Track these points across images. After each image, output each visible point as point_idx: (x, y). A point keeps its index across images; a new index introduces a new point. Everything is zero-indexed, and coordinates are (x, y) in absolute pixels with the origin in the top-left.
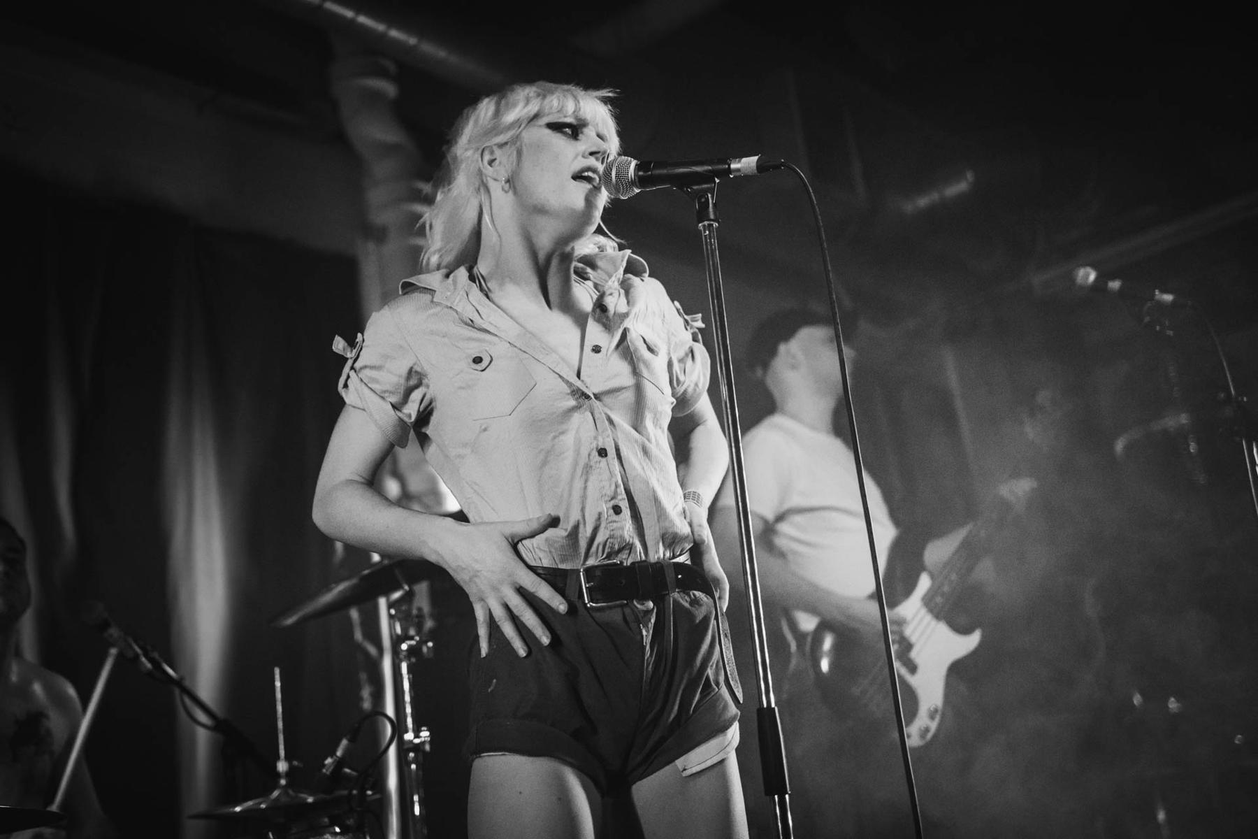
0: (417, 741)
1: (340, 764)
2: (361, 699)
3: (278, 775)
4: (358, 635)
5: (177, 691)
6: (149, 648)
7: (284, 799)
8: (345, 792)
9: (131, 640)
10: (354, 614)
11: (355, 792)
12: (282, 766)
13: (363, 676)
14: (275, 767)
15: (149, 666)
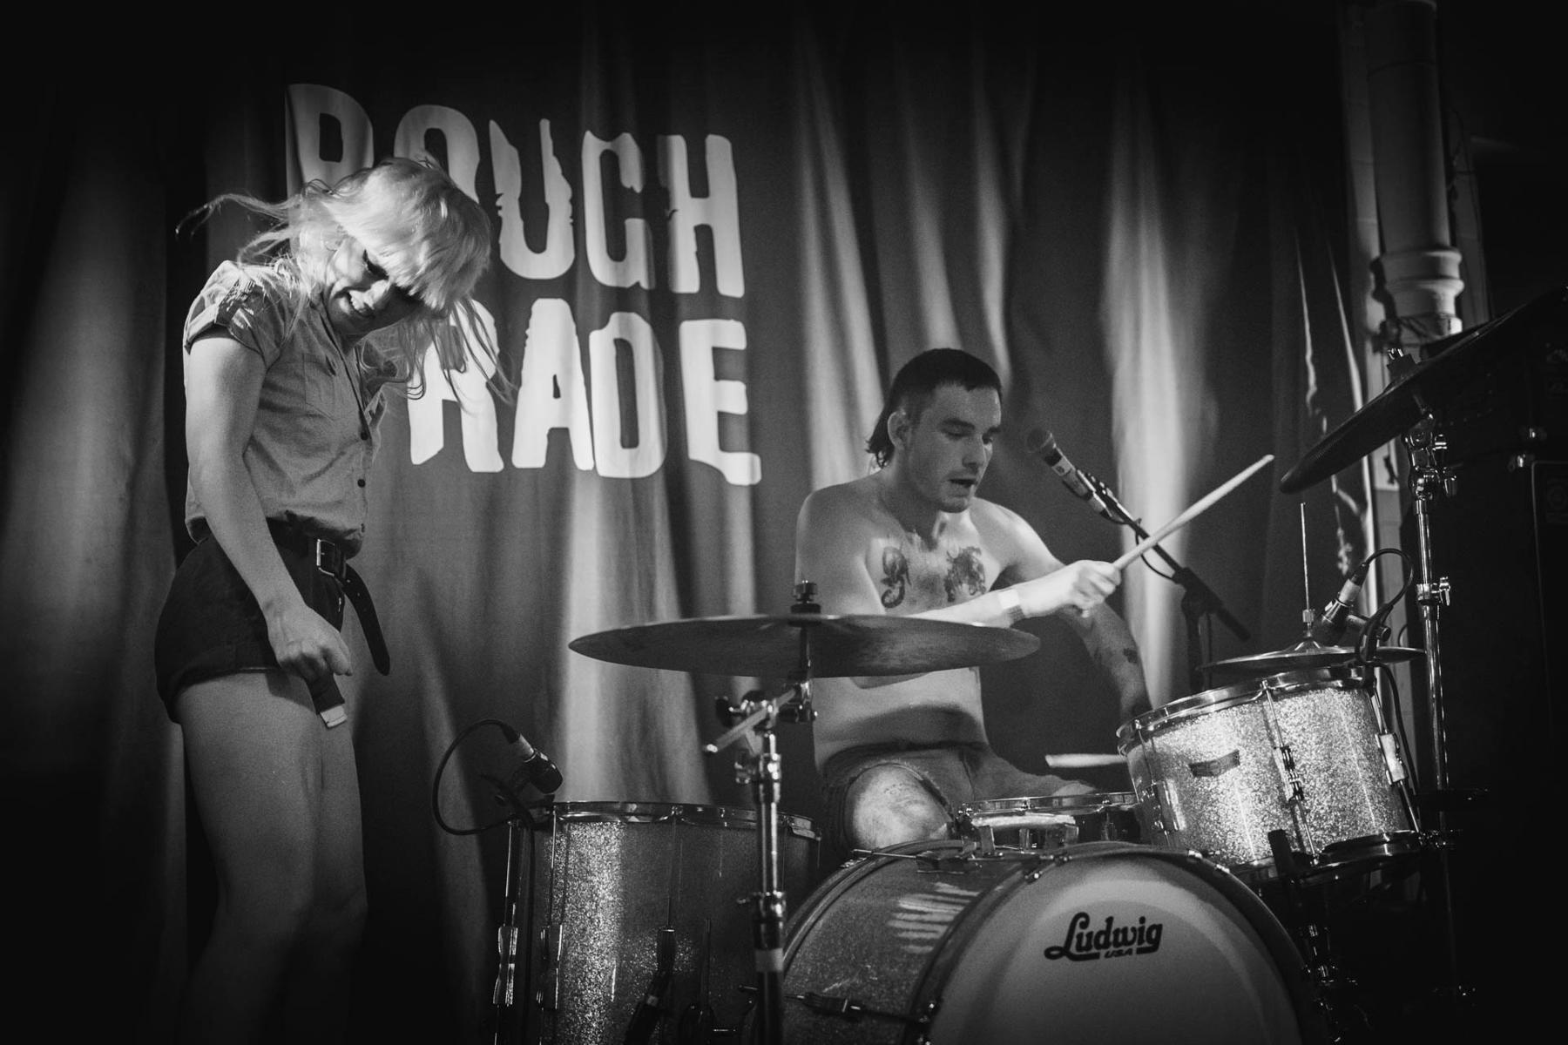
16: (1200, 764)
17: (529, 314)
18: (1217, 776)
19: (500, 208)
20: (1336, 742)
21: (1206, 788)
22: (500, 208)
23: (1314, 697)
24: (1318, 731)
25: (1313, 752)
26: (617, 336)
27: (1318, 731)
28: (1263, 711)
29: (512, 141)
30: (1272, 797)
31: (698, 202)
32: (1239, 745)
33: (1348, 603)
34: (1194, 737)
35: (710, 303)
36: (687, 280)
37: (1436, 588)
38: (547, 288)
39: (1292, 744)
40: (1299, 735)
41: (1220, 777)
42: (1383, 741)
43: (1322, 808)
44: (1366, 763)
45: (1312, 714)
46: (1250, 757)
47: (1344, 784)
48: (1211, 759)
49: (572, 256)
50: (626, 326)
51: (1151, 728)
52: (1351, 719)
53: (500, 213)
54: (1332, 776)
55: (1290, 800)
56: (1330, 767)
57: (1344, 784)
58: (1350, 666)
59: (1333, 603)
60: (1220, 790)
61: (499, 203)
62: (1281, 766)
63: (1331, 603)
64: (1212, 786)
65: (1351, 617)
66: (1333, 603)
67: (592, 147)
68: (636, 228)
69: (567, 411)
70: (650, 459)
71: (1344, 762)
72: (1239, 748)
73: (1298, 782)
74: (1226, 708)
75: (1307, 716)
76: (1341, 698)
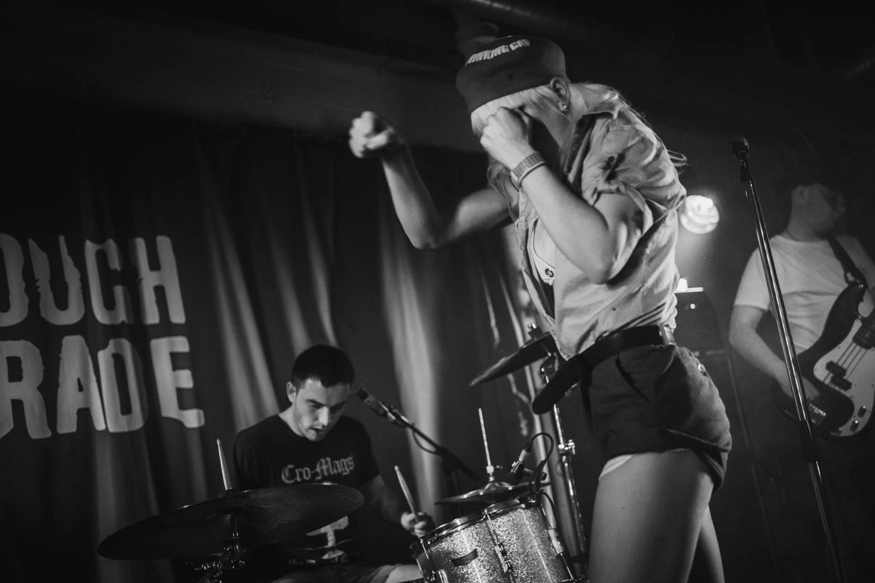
0: (566, 449)
1: (521, 467)
2: (520, 429)
3: (489, 475)
4: (514, 390)
5: (410, 431)
6: (392, 407)
7: (492, 489)
8: (527, 483)
9: (381, 403)
10: (511, 377)
11: (533, 483)
12: (490, 469)
13: (520, 415)
14: (486, 470)
15: (393, 418)
16: (458, 559)
17: (61, 345)
18: (467, 564)
19: (38, 287)
20: (526, 537)
21: (461, 572)
22: (38, 287)
23: (513, 515)
24: (516, 533)
25: (515, 545)
26: (114, 351)
27: (516, 533)
28: (487, 526)
29: (43, 249)
30: (497, 572)
31: (154, 274)
32: (476, 546)
33: (523, 462)
34: (452, 545)
35: (167, 328)
36: (152, 317)
37: (567, 446)
38: (71, 330)
39: (504, 542)
40: (507, 537)
41: (468, 565)
42: (549, 533)
43: (524, 575)
44: (542, 547)
45: (512, 524)
46: (483, 552)
47: (533, 559)
48: (463, 555)
49: (83, 311)
50: (118, 346)
51: (429, 543)
52: (532, 524)
53: (39, 290)
54: (526, 556)
55: (506, 572)
56: (525, 552)
57: (533, 559)
58: (528, 495)
59: (516, 462)
60: (469, 572)
61: (38, 284)
62: (500, 555)
63: (515, 462)
64: (465, 570)
65: (526, 469)
66: (516, 462)
67: (90, 249)
68: (119, 290)
69: (88, 398)
70: (137, 421)
71: (532, 547)
72: (476, 547)
73: (509, 562)
74: (467, 527)
75: (510, 525)
76: (526, 513)
